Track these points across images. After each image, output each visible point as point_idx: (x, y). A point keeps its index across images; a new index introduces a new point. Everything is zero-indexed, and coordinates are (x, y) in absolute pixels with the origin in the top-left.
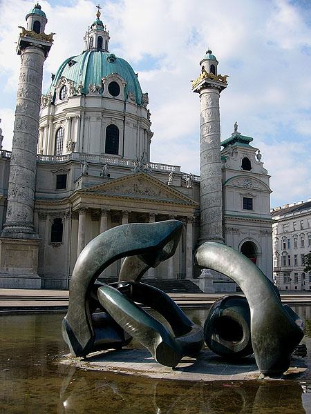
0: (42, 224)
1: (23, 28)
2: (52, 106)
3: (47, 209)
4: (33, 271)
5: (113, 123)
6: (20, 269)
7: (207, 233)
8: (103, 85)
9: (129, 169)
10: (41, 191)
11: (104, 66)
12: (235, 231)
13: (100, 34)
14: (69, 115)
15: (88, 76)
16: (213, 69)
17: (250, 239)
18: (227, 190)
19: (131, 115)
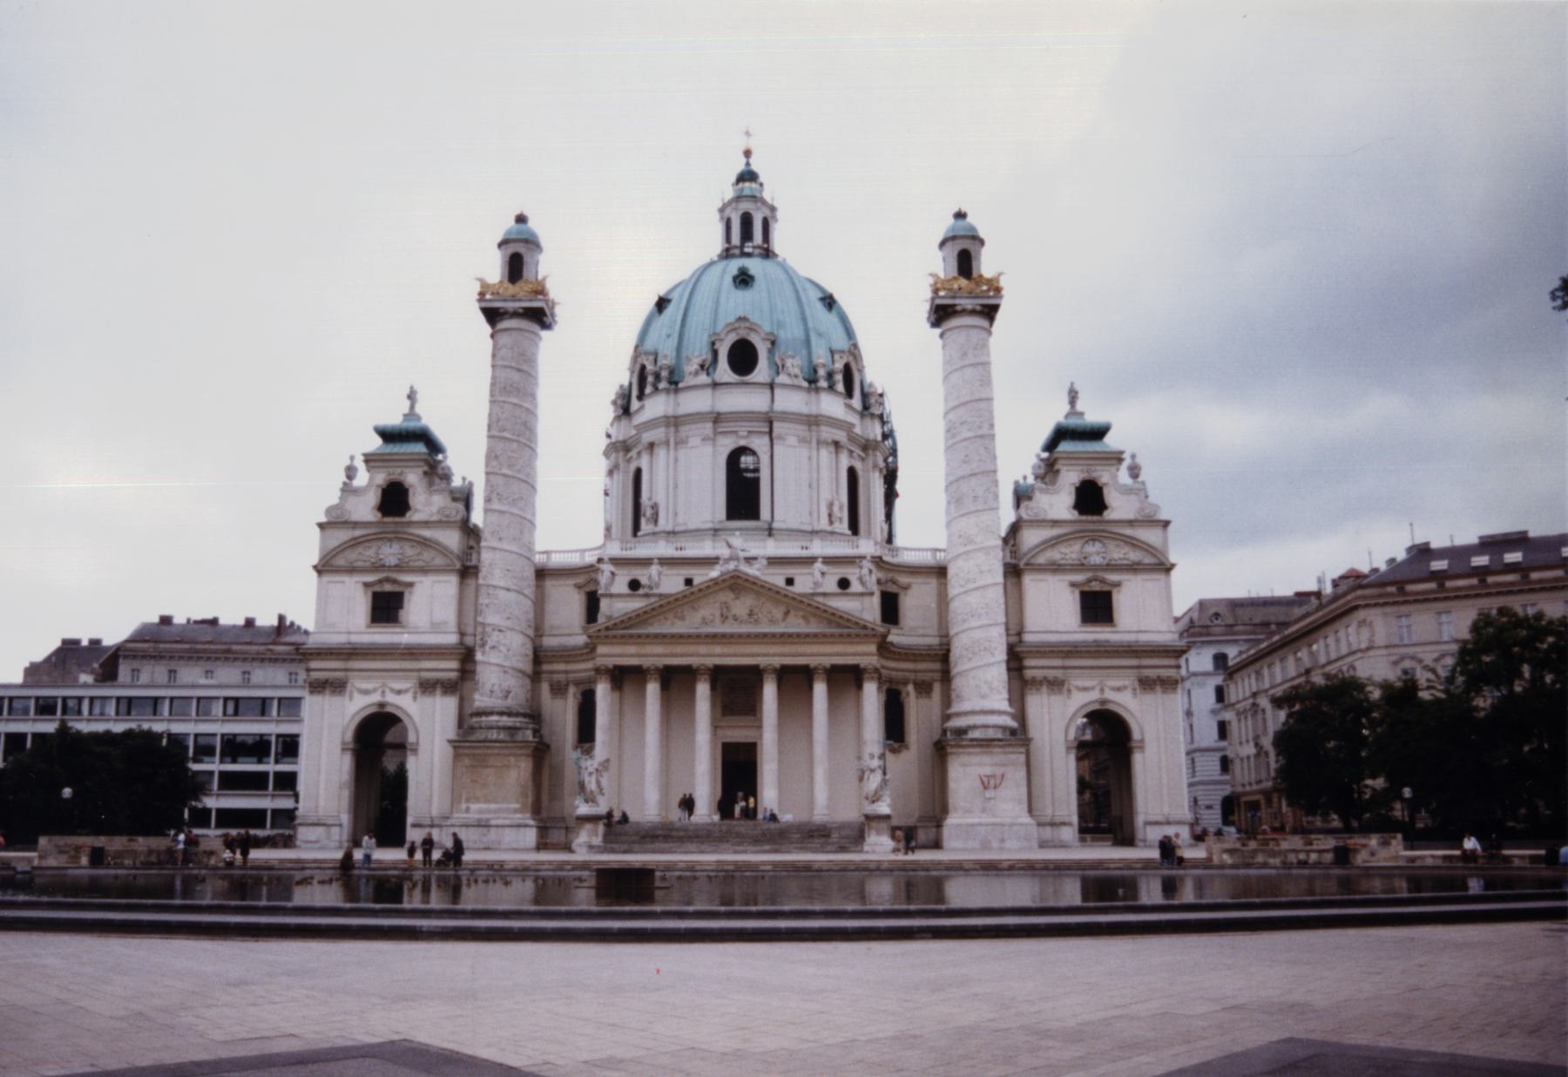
0: (558, 703)
1: (481, 280)
2: (624, 422)
3: (567, 672)
5: (742, 443)
8: (715, 353)
11: (723, 299)
12: (1056, 685)
13: (746, 206)
14: (647, 437)
16: (965, 263)
17: (1104, 702)
18: (1028, 580)
19: (787, 417)
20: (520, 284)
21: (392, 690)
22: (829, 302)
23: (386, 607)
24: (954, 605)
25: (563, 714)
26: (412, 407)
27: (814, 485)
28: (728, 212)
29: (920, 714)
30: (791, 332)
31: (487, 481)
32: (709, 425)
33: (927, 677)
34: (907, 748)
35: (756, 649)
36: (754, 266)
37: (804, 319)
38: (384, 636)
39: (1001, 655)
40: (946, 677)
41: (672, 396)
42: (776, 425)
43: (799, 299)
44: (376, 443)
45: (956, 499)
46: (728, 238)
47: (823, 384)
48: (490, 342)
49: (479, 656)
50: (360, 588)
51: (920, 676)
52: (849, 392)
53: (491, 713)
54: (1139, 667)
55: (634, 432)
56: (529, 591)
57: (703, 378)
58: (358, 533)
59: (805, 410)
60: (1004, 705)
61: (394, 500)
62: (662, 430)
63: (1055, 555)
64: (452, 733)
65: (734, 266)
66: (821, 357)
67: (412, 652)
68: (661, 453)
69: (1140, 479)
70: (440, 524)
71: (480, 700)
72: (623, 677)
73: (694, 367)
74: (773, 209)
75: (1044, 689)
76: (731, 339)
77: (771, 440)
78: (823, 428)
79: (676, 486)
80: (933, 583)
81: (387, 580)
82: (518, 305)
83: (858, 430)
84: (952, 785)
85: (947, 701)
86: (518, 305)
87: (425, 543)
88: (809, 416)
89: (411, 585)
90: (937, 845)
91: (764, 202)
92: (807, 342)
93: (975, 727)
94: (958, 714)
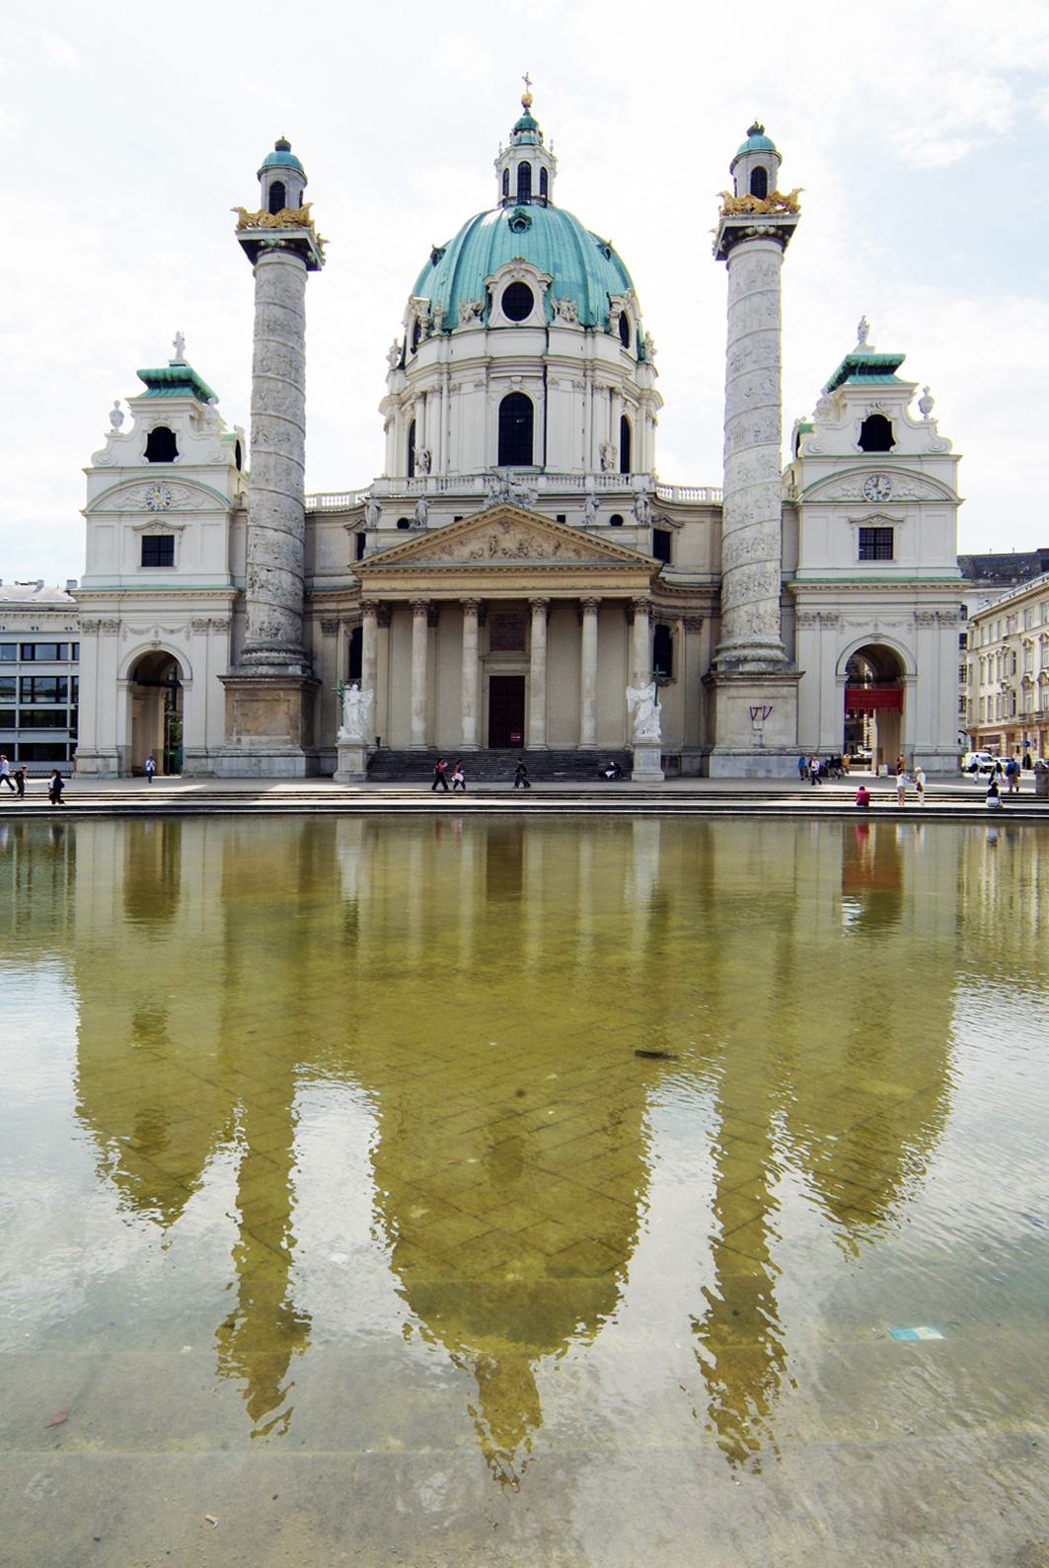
0: (330, 642)
1: (241, 211)
3: (339, 611)
4: (292, 742)
5: (516, 388)
6: (264, 738)
7: (730, 633)
8: (490, 297)
9: (477, 499)
10: (326, 572)
12: (828, 620)
13: (524, 154)
15: (460, 283)
17: (877, 637)
18: (805, 515)
19: (563, 361)
20: (283, 213)
21: (164, 630)
22: (607, 251)
23: (158, 551)
24: (726, 543)
25: (334, 649)
26: (179, 354)
27: (588, 431)
28: (503, 167)
29: (690, 650)
30: (570, 274)
31: (253, 422)
32: (484, 370)
33: (697, 614)
34: (674, 681)
35: (524, 582)
36: (532, 210)
37: (582, 263)
38: (157, 576)
39: (775, 590)
40: (717, 613)
41: (445, 342)
42: (549, 368)
43: (577, 245)
44: (144, 388)
45: (736, 434)
46: (505, 190)
47: (601, 329)
48: (253, 280)
49: (249, 595)
50: (130, 531)
51: (690, 614)
52: (626, 344)
53: (261, 650)
54: (916, 603)
55: (409, 383)
56: (299, 532)
57: (476, 323)
58: (124, 478)
59: (580, 355)
60: (776, 640)
61: (161, 445)
62: (436, 376)
63: (835, 492)
64: (223, 668)
65: (508, 214)
66: (598, 303)
67: (182, 593)
68: (433, 401)
69: (931, 415)
70: (213, 467)
71: (249, 638)
72: (389, 612)
73: (469, 312)
74: (552, 160)
75: (817, 625)
76: (506, 282)
77: (545, 385)
78: (598, 372)
79: (449, 433)
80: (708, 520)
81: (156, 524)
82: (281, 235)
83: (632, 378)
84: (720, 716)
85: (717, 636)
86: (281, 235)
87: (195, 486)
88: (584, 361)
89: (182, 529)
90: (702, 774)
91: (542, 151)
92: (585, 287)
93: (745, 660)
94: (728, 649)
